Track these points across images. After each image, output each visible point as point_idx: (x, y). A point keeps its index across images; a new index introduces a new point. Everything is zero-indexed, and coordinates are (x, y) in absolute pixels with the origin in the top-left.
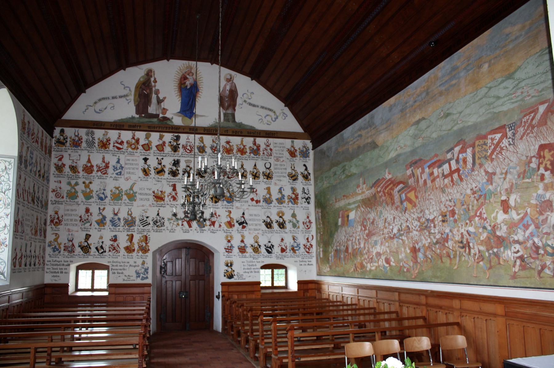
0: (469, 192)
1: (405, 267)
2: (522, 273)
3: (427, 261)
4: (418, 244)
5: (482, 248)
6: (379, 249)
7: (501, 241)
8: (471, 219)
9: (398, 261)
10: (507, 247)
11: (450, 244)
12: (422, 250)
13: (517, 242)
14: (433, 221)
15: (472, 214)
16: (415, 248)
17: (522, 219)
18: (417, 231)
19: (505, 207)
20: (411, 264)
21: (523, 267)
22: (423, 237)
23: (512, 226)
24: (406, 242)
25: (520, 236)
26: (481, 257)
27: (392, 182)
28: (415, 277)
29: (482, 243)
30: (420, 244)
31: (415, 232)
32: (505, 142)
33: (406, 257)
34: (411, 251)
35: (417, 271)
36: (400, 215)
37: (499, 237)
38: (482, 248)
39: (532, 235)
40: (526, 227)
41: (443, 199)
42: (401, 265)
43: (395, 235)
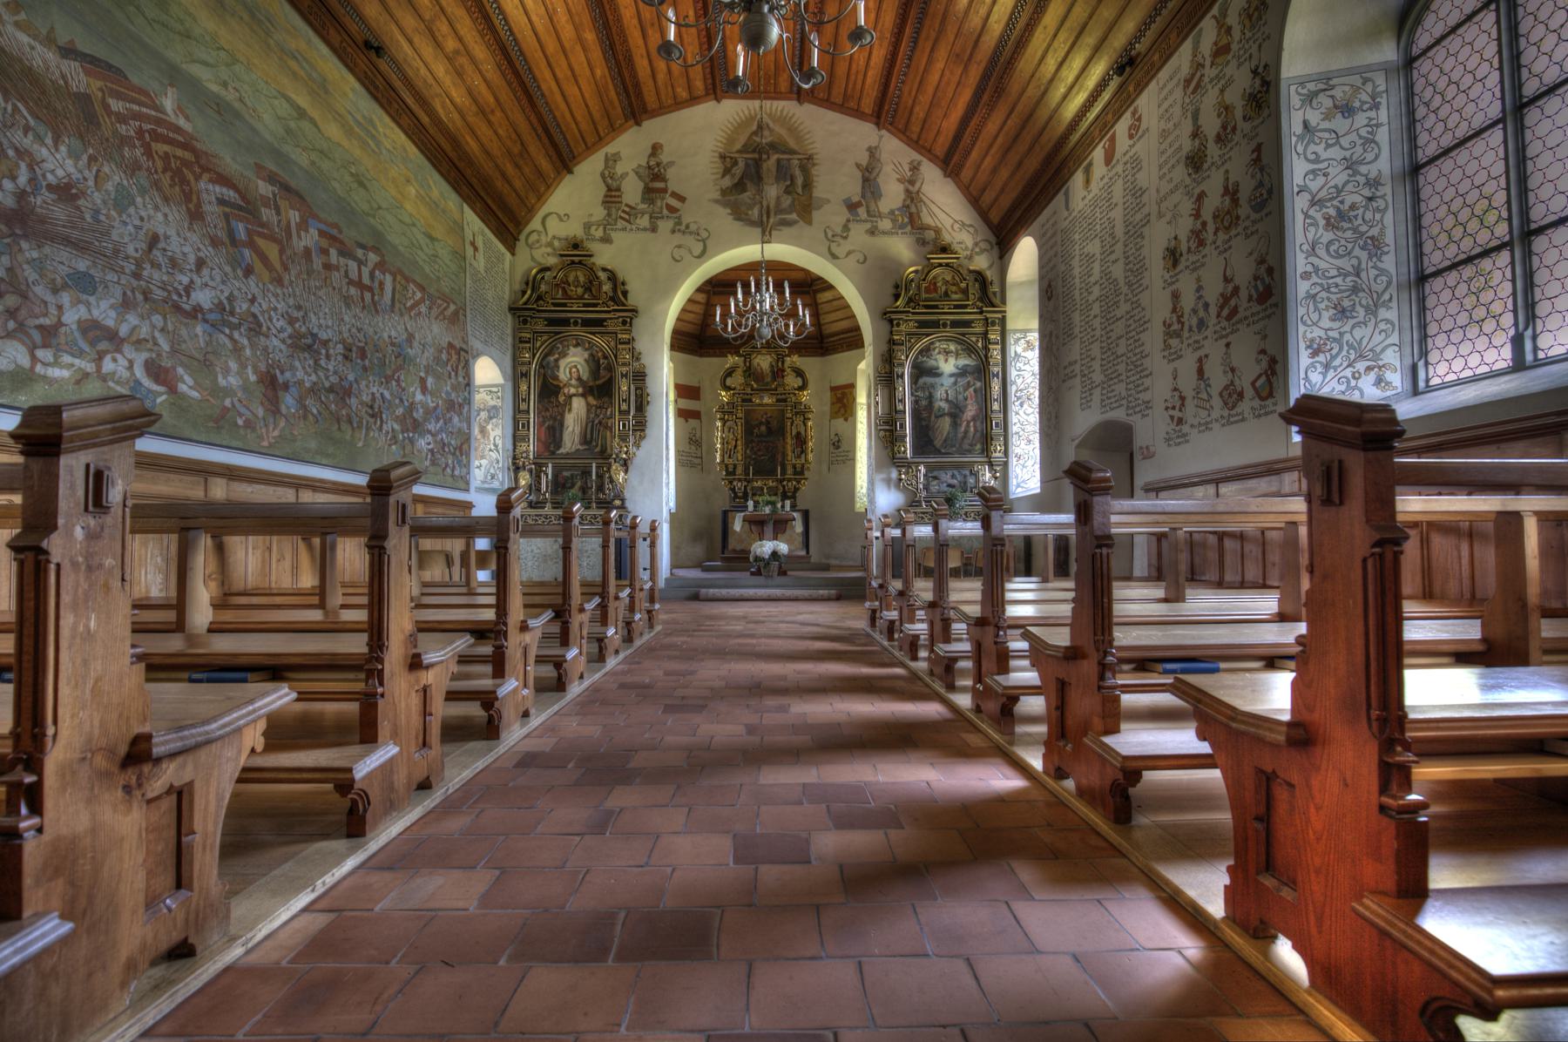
0: (385, 335)
1: (241, 415)
2: (431, 469)
3: (305, 417)
4: (282, 372)
5: (396, 427)
6: (103, 311)
7: (417, 426)
8: (388, 379)
9: (217, 392)
10: (422, 435)
11: (353, 401)
12: (293, 390)
13: (429, 432)
14: (325, 343)
15: (389, 372)
16: (273, 379)
17: (435, 408)
18: (283, 341)
19: (424, 390)
20: (260, 412)
21: (433, 463)
22: (297, 364)
23: (429, 412)
24: (248, 352)
25: (431, 426)
26: (394, 439)
27: (193, 150)
28: (271, 445)
29: (397, 419)
30: (288, 375)
31: (276, 342)
32: (423, 309)
33: (245, 388)
34: (261, 381)
35: (276, 433)
36: (228, 269)
37: (415, 420)
38: (396, 427)
39: (441, 430)
40: (438, 420)
41: (346, 318)
42: (228, 403)
43: (197, 309)
